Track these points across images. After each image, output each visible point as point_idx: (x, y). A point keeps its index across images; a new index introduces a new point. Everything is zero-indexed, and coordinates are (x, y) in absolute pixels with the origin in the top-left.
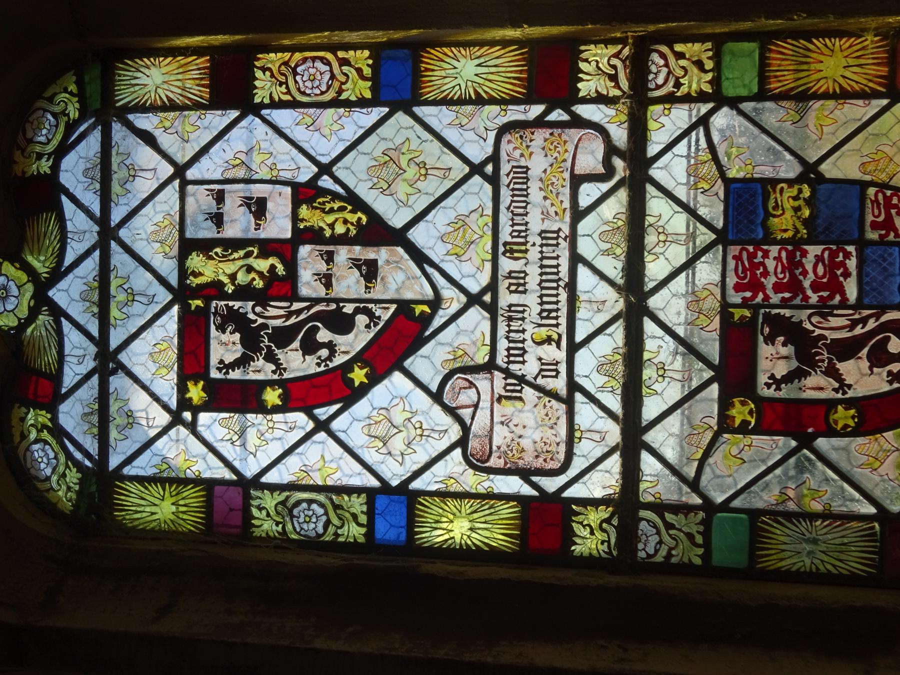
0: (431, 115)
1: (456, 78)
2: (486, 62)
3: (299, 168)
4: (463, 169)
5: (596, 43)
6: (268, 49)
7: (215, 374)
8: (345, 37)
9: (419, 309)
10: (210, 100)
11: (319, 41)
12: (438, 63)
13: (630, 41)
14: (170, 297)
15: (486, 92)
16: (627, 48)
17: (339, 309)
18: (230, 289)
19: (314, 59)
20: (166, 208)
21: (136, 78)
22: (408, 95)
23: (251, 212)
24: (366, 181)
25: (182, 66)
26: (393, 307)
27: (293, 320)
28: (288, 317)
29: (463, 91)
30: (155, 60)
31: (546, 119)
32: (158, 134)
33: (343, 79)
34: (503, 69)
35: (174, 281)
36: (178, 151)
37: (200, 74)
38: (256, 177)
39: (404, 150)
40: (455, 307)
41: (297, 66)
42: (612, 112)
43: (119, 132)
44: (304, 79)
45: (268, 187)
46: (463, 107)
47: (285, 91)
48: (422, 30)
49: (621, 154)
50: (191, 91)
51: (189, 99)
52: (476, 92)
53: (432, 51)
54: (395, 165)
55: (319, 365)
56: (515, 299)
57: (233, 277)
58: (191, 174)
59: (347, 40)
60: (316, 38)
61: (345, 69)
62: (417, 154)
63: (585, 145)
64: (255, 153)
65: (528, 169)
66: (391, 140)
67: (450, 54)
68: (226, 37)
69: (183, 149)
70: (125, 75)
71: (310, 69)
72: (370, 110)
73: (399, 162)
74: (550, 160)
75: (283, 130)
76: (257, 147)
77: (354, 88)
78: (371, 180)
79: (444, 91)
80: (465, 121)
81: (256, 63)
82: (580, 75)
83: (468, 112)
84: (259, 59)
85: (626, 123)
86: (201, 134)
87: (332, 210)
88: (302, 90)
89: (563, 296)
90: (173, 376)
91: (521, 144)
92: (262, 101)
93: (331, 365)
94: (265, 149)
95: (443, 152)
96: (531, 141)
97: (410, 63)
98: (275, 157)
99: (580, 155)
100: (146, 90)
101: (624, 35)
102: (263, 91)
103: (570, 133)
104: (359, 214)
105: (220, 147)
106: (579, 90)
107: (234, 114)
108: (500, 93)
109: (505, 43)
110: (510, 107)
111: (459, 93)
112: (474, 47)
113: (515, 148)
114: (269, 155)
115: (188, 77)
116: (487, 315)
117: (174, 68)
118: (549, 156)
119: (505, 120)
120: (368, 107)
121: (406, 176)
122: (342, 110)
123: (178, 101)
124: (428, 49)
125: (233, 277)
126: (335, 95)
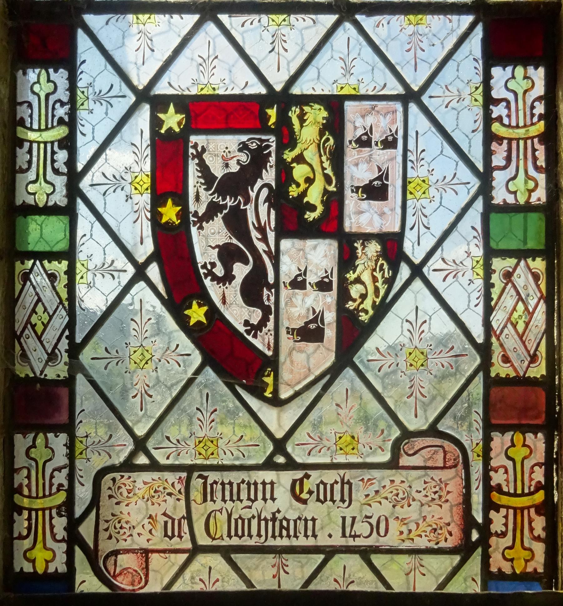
87: (375, 279)
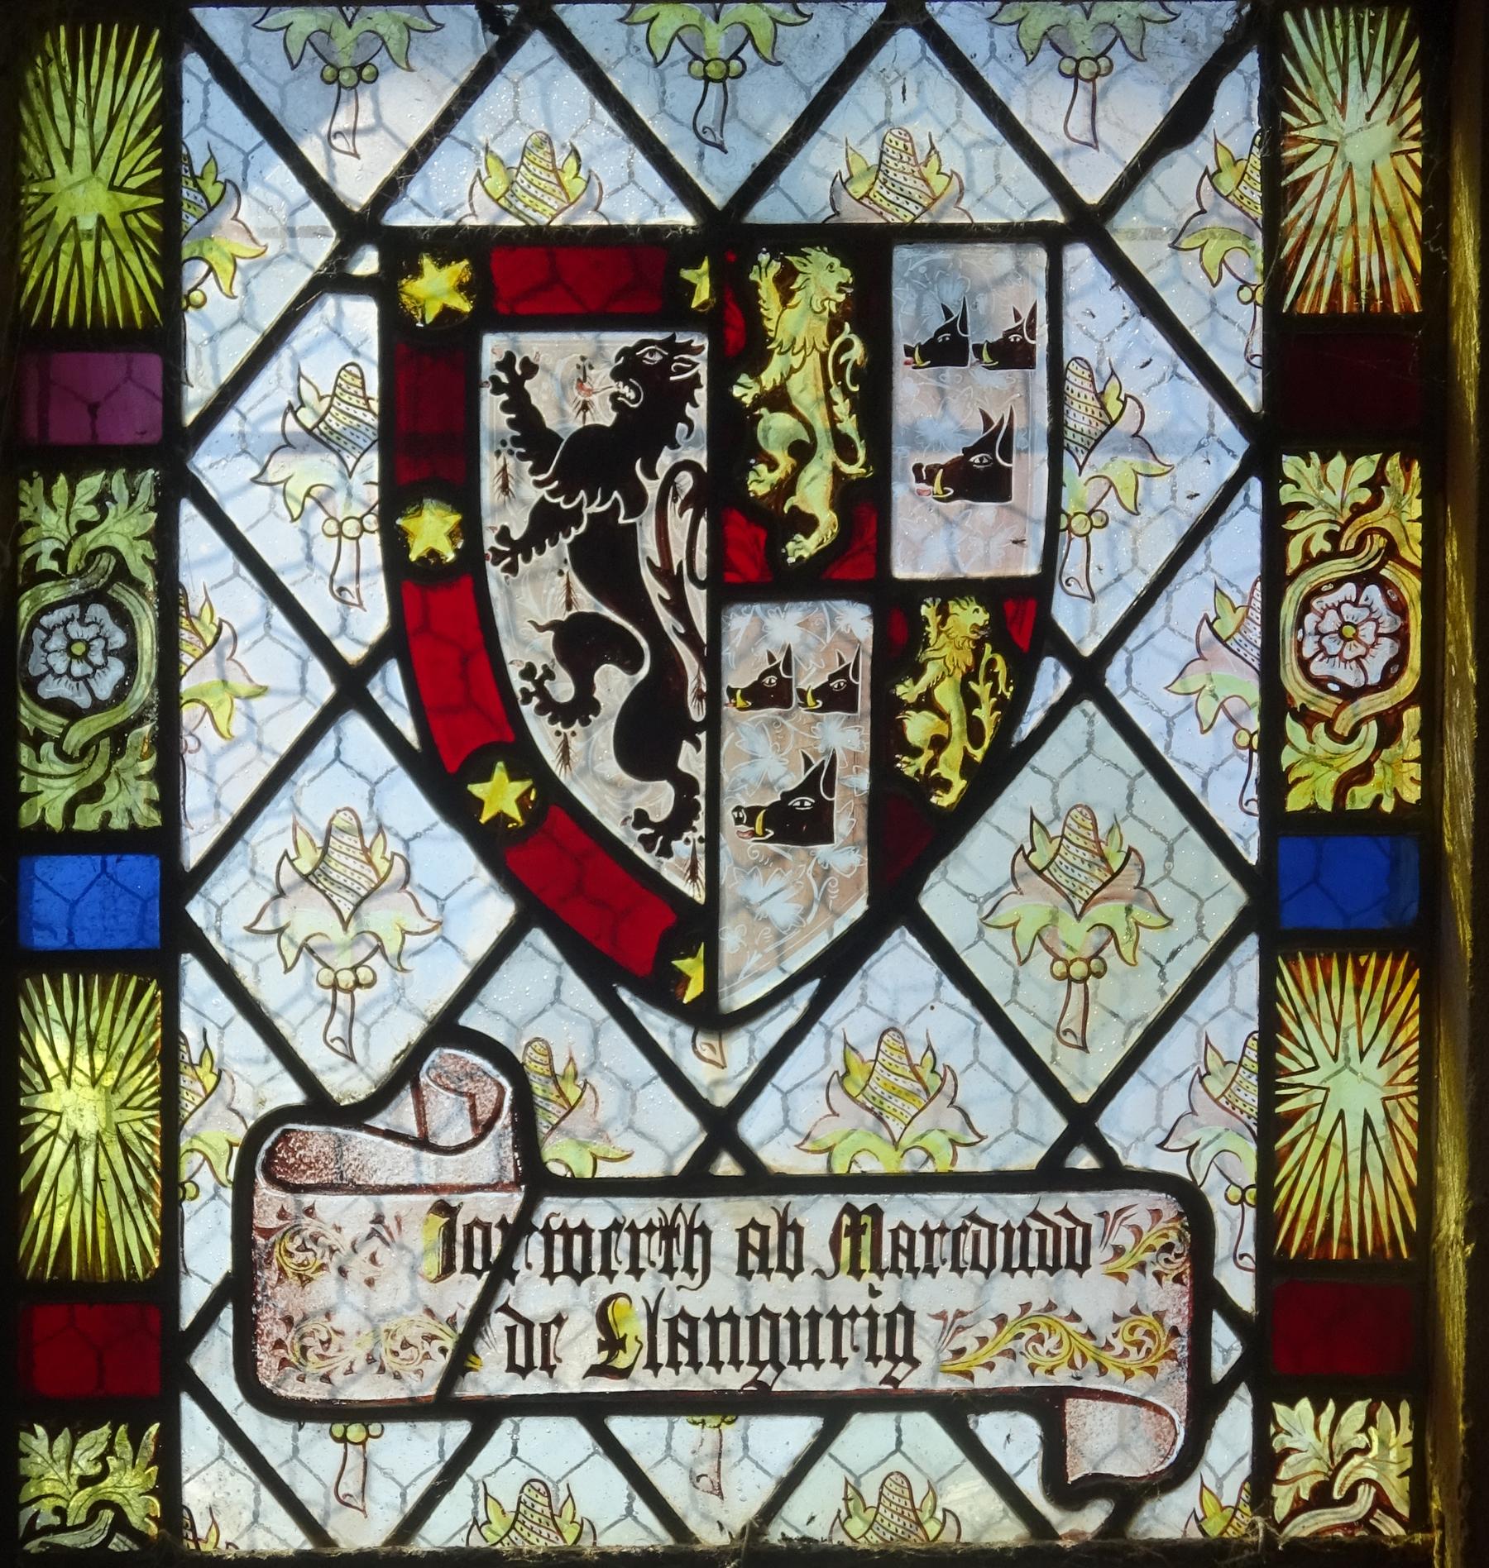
0: (1234, 988)
1: (1335, 1058)
2: (1376, 1141)
3: (1093, 598)
4: (1082, 1085)
5: (1417, 1445)
6: (1434, 495)
7: (493, 347)
8: (1459, 730)
9: (692, 968)
10: (1294, 318)
11: (1451, 649)
12: (1377, 1004)
13: (1419, 1538)
14: (718, 200)
15: (1294, 1143)
16: (1400, 1531)
17: (689, 731)
18: (744, 391)
19: (1401, 636)
20: (982, 181)
21: (1365, 76)
22: (1291, 918)
23: (969, 452)
24: (1054, 801)
25: (1394, 225)
26: (697, 893)
27: (655, 590)
28: (666, 575)
29: (1297, 1079)
30: (1415, 138)
31: (1215, 1314)
32: (1200, 151)
33: (1342, 726)
34: (1354, 1191)
35: (767, 211)
36: (1147, 218)
37: (1370, 284)
38: (1069, 464)
39: (1138, 911)
40: (698, 1072)
41: (1384, 584)
42: (1230, 1496)
43: (1208, 23)
44: (1347, 609)
45: (1039, 506)
46: (1254, 1079)
47: (1314, 552)
48: (1469, 955)
49: (1117, 1524)
50: (1322, 256)
51: (1299, 250)
52: (1296, 1115)
53: (1411, 987)
54: (1096, 885)
55: (528, 672)
56: (725, 1244)
57: (779, 399)
58: (1080, 259)
59: (1451, 733)
60: (1461, 642)
61: (1371, 731)
62: (1127, 950)
63: (1142, 1426)
64: (1137, 461)
65: (1081, 1269)
66: (1167, 874)
67: (1401, 1039)
68: (1474, 362)
69: (1153, 234)
70: (1373, 39)
71: (1371, 626)
72: (1254, 807)
73: (1106, 898)
74: (1105, 1331)
75: (1202, 546)
76: (1155, 468)
77: (1315, 759)
78: (1057, 817)
79: (1300, 1025)
80: (1215, 1086)
81: (1395, 459)
82: (1331, 1406)
83: (1241, 1094)
84: (1406, 467)
85: (1199, 1535)
86: (1196, 290)
87: (970, 700)
88: (1314, 603)
89: (733, 1380)
90: (483, 215)
91: (1151, 1248)
92: (1287, 480)
93: (528, 710)
94: (1148, 491)
95: (1131, 1026)
96: (1158, 1276)
97: (1382, 923)
98: (1124, 523)
99: (1116, 1413)
100: (1329, 110)
101: (1435, 1521)
102: (1314, 482)
103: (1176, 1383)
104: (959, 785)
105: (1158, 352)
106: (1292, 1404)
107: (1251, 394)
108: (1289, 1183)
109: (1425, 1193)
110: (1251, 1213)
111: (1294, 1067)
112: (1418, 1107)
113: (1138, 1231)
114: (1131, 507)
115: (1363, 244)
116: (679, 1166)
117: (1391, 201)
118: (1115, 1327)
119: (1216, 1201)
120: (1263, 803)
121: (1067, 918)
122: (1254, 724)
123: (1292, 214)
124: (1417, 975)
125: (779, 399)
126: (1298, 704)
